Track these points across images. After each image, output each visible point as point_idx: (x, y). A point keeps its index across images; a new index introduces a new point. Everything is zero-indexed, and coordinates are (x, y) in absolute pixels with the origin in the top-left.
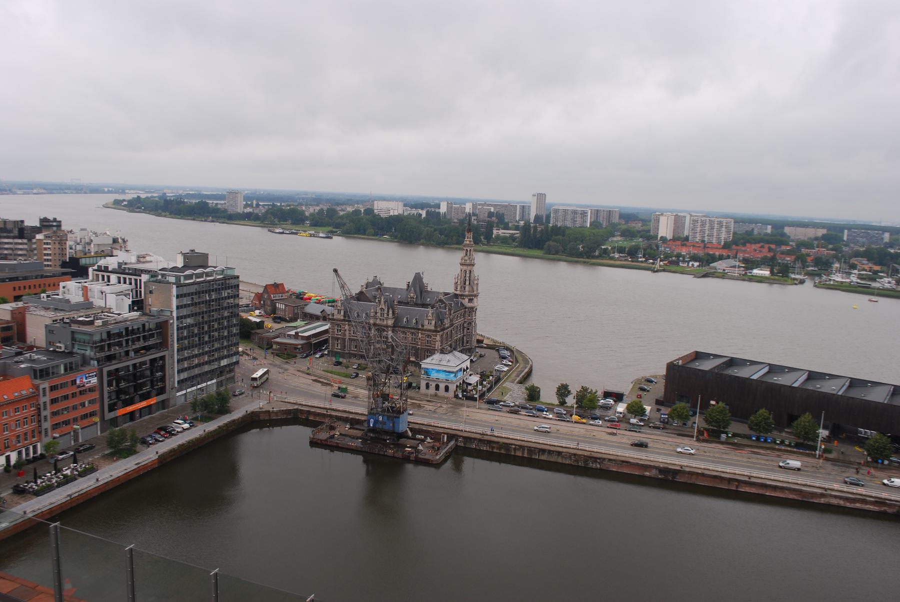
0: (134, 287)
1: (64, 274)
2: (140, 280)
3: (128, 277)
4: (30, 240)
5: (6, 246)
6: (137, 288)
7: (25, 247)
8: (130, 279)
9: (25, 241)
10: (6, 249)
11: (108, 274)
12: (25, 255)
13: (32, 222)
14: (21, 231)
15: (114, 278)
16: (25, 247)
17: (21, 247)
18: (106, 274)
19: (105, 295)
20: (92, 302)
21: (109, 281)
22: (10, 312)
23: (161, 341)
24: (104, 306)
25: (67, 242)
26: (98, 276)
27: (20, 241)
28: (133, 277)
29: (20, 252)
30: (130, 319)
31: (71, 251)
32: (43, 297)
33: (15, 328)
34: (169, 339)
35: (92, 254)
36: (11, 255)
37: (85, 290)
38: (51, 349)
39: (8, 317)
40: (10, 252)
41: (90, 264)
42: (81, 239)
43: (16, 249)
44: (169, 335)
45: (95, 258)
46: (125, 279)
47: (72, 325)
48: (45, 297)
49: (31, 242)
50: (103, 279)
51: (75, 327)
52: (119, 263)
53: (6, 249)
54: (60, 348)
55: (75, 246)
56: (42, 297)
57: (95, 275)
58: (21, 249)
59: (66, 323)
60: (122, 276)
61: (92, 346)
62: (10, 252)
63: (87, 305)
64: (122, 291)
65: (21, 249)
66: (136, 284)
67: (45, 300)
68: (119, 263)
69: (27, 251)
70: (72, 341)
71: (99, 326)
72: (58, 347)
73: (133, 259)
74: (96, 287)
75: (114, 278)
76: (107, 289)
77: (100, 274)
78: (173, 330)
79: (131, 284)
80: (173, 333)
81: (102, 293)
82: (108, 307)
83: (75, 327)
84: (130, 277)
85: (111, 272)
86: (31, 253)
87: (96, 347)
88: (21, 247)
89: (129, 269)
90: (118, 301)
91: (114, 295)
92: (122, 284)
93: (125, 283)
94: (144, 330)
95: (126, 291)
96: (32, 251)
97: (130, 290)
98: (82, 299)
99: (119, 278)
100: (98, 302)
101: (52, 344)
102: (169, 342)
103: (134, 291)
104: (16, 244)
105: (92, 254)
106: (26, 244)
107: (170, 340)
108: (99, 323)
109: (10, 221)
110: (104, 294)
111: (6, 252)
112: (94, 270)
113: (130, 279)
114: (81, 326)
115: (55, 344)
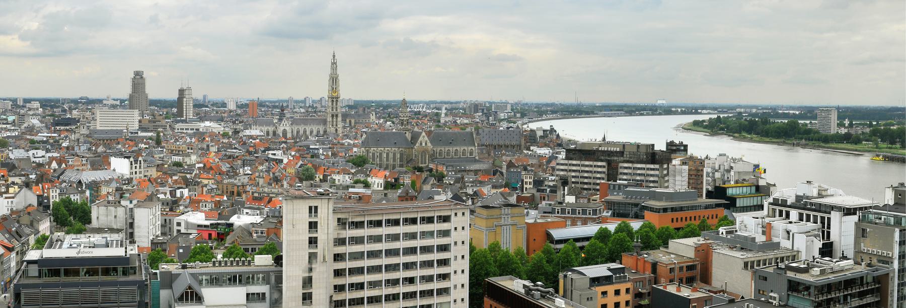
0: (821, 227)
1: (718, 205)
2: (829, 219)
3: (812, 213)
4: (661, 166)
5: (639, 172)
6: (823, 227)
7: (657, 172)
8: (815, 217)
9: (657, 166)
10: (640, 175)
11: (788, 209)
12: (656, 182)
13: (661, 146)
14: (652, 156)
15: (794, 215)
16: (657, 172)
17: (652, 172)
18: (784, 209)
19: (793, 235)
20: (779, 243)
21: (788, 216)
22: (694, 249)
23: (879, 299)
24: (791, 248)
25: (705, 169)
26: (774, 210)
27: (652, 166)
28: (819, 215)
29: (652, 179)
30: (846, 268)
31: (709, 178)
32: (722, 233)
33: (699, 267)
34: (889, 297)
35: (732, 183)
36: (642, 181)
37: (767, 229)
38: (763, 299)
39: (691, 254)
40: (642, 178)
41: (739, 195)
42: (720, 165)
43: (648, 175)
44: (889, 292)
45: (741, 188)
46: (808, 216)
47: (788, 272)
48: (724, 233)
49: (663, 168)
50: (781, 215)
51: (790, 274)
52: (797, 197)
53: (640, 175)
54: (775, 299)
55: (713, 173)
56: (720, 233)
57: (771, 210)
58: (652, 175)
59: (781, 268)
60: (805, 212)
61: (813, 300)
62: (642, 178)
63: (771, 246)
64: (808, 230)
65: (652, 175)
66: (823, 223)
67: (725, 236)
68: (797, 197)
69: (659, 178)
70: (788, 291)
71: (818, 276)
72: (771, 298)
73: (815, 194)
74: (779, 225)
75: (794, 215)
76: (790, 227)
77: (778, 208)
78: (893, 287)
79: (815, 222)
80: (893, 291)
81: (788, 232)
82: (795, 249)
83: (790, 274)
84: (816, 214)
85: (790, 207)
86: (662, 180)
87: (815, 302)
88: (652, 172)
89: (811, 204)
90: (808, 243)
91: (804, 236)
92: (804, 222)
93: (808, 220)
94: (862, 284)
95: (812, 230)
96: (663, 178)
97: (817, 230)
98: (764, 238)
99: (801, 215)
100: (786, 244)
101: (761, 292)
102: (889, 301)
103: (820, 231)
104: (648, 169)
105: (732, 183)
106: (657, 170)
107: (890, 299)
108: (816, 271)
109: (642, 145)
110: (791, 234)
111: (638, 178)
112: (770, 204)
113: (815, 217)
114: (798, 274)
115: (765, 293)
